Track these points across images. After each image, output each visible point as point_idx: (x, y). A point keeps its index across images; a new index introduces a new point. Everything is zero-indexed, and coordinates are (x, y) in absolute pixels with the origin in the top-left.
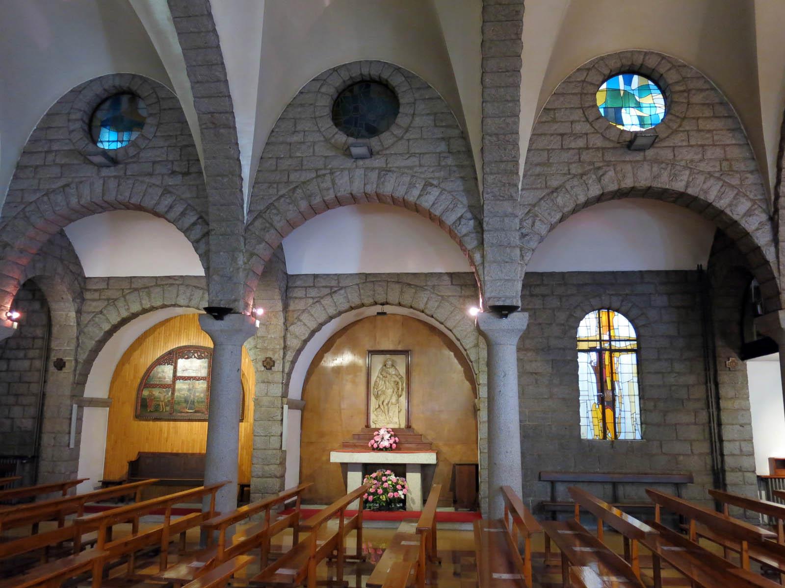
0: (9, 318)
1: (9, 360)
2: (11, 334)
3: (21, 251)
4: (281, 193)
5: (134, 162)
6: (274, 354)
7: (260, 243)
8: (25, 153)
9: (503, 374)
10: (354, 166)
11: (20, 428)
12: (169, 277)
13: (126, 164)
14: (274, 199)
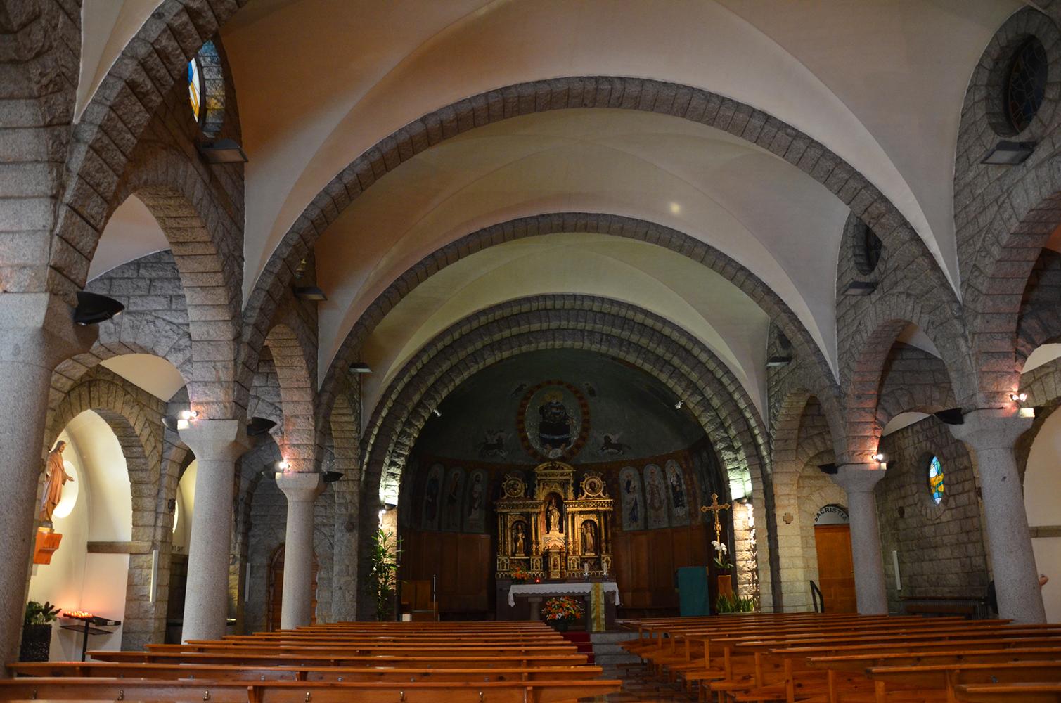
0: (878, 461)
1: (954, 495)
2: (883, 476)
3: (859, 397)
4: (977, 248)
5: (885, 277)
7: (975, 318)
8: (839, 304)
10: (1025, 171)
11: (976, 566)
13: (882, 281)
14: (974, 258)
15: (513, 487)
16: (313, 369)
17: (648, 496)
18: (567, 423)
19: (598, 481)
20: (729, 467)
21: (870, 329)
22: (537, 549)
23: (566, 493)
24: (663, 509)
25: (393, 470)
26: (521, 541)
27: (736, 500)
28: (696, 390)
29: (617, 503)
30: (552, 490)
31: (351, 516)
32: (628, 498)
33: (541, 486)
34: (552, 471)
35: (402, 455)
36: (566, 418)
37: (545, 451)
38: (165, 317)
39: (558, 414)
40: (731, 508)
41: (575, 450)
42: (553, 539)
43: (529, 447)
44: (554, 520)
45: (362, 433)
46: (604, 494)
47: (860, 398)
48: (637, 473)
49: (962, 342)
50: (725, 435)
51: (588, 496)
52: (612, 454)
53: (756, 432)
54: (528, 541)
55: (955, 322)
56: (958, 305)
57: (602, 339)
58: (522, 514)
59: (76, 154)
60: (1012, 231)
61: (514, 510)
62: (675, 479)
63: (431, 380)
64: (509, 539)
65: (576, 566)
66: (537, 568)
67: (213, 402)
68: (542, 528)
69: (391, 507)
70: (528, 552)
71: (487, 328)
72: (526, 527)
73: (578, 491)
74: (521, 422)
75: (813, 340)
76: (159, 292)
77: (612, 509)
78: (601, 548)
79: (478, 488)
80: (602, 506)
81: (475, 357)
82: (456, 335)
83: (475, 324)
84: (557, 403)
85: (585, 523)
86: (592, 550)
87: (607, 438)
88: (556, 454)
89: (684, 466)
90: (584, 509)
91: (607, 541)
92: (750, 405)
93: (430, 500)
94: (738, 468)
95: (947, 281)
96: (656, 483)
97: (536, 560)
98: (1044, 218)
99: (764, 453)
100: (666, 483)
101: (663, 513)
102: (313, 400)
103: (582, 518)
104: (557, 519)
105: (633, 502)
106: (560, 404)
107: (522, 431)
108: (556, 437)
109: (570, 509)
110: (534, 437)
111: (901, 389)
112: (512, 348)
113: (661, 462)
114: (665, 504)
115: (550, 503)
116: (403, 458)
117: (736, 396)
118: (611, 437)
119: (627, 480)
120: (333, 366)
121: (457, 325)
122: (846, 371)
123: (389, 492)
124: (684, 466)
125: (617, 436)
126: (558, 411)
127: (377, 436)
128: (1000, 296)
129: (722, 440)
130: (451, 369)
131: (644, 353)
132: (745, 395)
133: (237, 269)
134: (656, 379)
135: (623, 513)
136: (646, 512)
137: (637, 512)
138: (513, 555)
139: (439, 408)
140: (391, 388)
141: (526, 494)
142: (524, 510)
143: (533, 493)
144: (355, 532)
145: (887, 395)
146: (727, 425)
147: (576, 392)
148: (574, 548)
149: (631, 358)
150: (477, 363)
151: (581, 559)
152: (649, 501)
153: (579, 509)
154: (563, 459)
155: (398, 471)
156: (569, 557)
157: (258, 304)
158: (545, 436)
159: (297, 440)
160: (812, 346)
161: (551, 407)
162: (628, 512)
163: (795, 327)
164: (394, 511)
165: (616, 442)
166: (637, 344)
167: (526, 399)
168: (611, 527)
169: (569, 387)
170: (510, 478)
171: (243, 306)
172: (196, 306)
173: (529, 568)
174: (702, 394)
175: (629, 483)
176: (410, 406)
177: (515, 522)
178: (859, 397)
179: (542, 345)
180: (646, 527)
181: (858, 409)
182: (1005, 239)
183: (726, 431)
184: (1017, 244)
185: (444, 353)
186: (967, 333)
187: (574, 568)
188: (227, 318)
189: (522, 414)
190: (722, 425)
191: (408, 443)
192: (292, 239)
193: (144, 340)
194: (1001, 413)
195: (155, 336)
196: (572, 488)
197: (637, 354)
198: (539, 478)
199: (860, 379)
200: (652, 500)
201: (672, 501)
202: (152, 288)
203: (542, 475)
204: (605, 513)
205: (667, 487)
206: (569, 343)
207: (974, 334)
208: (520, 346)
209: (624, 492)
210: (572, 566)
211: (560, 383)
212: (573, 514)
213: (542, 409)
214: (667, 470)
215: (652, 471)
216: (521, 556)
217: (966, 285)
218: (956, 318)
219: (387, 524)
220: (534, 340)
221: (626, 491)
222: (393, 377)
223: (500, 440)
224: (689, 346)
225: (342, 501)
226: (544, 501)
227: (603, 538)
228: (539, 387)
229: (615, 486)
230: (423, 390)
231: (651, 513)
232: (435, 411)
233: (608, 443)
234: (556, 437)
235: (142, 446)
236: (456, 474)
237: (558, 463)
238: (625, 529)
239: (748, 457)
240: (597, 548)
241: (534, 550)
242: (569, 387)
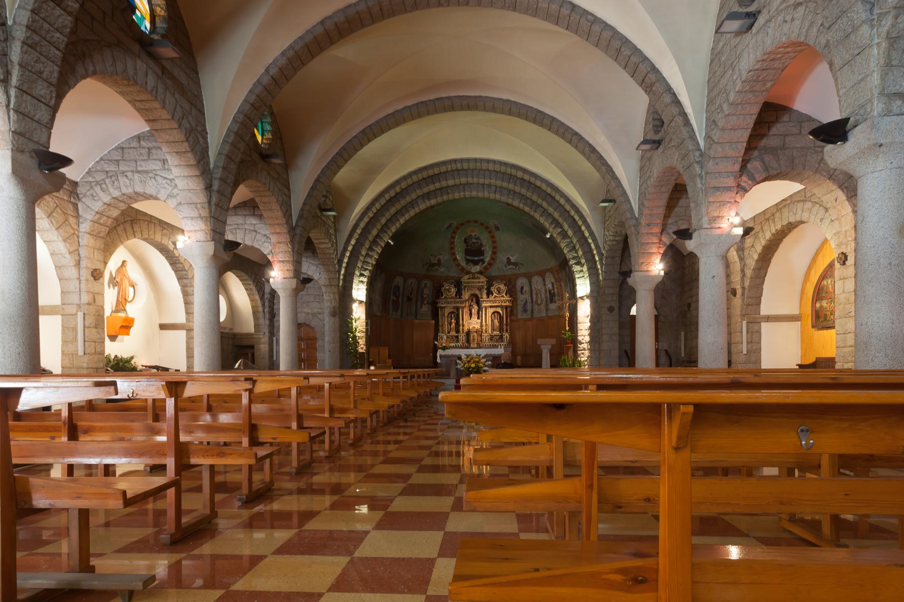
6: (846, 248)
9: (861, 219)
12: (783, 200)
15: (449, 290)
16: (287, 211)
17: (534, 296)
19: (502, 287)
20: (577, 276)
21: (655, 175)
22: (463, 329)
23: (481, 294)
24: (543, 305)
25: (362, 279)
26: (454, 324)
27: (580, 298)
28: (558, 224)
29: (514, 300)
30: (473, 292)
31: (334, 307)
32: (521, 297)
33: (466, 290)
34: (473, 280)
35: (367, 269)
36: (481, 245)
37: (469, 267)
38: (162, 174)
39: (476, 243)
40: (577, 302)
41: (488, 267)
42: (472, 323)
43: (459, 265)
44: (474, 311)
45: (339, 255)
46: (506, 294)
47: (650, 225)
48: (527, 281)
49: (698, 180)
50: (576, 255)
51: (495, 296)
53: (595, 252)
54: (457, 324)
55: (696, 165)
56: (699, 152)
57: (496, 190)
58: (454, 307)
59: (14, 48)
60: (736, 90)
61: (449, 305)
62: (551, 285)
63: (383, 221)
64: (446, 323)
67: (198, 231)
68: (466, 317)
69: (361, 302)
70: (458, 331)
71: (419, 184)
72: (456, 315)
73: (489, 293)
74: (452, 248)
75: (622, 185)
76: (155, 157)
77: (511, 305)
78: (503, 329)
79: (426, 291)
81: (412, 204)
82: (398, 189)
83: (410, 181)
85: (494, 313)
87: (508, 259)
88: (476, 269)
89: (557, 277)
90: (493, 305)
91: (507, 325)
92: (592, 234)
93: (395, 299)
94: (583, 276)
95: (695, 133)
96: (539, 288)
97: (462, 337)
98: (761, 78)
99: (599, 267)
100: (545, 288)
101: (543, 307)
102: (289, 232)
103: (492, 310)
104: (476, 310)
107: (454, 254)
108: (476, 258)
109: (484, 305)
111: (683, 219)
112: (436, 198)
113: (542, 274)
114: (544, 302)
115: (472, 300)
116: (368, 271)
117: (583, 228)
118: (511, 258)
119: (521, 286)
120: (302, 210)
121: (398, 182)
122: (641, 207)
123: (359, 291)
124: (557, 277)
125: (515, 258)
127: (349, 257)
128: (728, 144)
129: (574, 258)
130: (396, 213)
131: (524, 199)
132: (588, 227)
133: (201, 139)
134: (533, 217)
136: (532, 307)
138: (449, 333)
139: (391, 238)
140: (356, 226)
141: (456, 295)
142: (455, 305)
143: (461, 295)
144: (337, 317)
145: (672, 224)
146: (577, 248)
147: (487, 228)
148: (486, 329)
149: (516, 203)
150: (414, 208)
152: (534, 300)
153: (490, 304)
154: (481, 273)
155: (365, 280)
156: (483, 334)
157: (221, 164)
158: (470, 258)
159: (282, 258)
160: (621, 189)
161: (472, 238)
163: (610, 176)
164: (364, 305)
166: (519, 193)
167: (455, 233)
168: (510, 317)
169: (482, 224)
171: (211, 166)
172: (176, 166)
173: (458, 341)
174: (561, 227)
175: (522, 288)
176: (371, 238)
177: (450, 313)
178: (649, 225)
179: (457, 196)
180: (532, 316)
181: (647, 233)
182: (732, 97)
183: (576, 252)
184: (742, 101)
185: (391, 201)
186: (703, 173)
188: (198, 174)
189: (452, 243)
190: (574, 248)
191: (371, 262)
192: (239, 118)
193: (150, 190)
194: (718, 232)
195: (157, 188)
196: (485, 291)
197: (519, 200)
199: (649, 212)
200: (537, 299)
201: (549, 300)
202: (151, 155)
204: (506, 307)
205: (546, 291)
206: (474, 194)
207: (707, 174)
208: (442, 196)
209: (519, 294)
211: (476, 222)
212: (486, 308)
213: (465, 239)
214: (546, 279)
215: (536, 279)
216: (453, 333)
217: (708, 137)
218: (697, 162)
219: (359, 313)
220: (451, 192)
221: (520, 293)
222: (357, 217)
223: (439, 260)
224: (553, 194)
225: (328, 298)
226: (468, 300)
227: (505, 322)
228: (462, 224)
229: (514, 290)
230: (379, 227)
231: (536, 307)
232: (390, 241)
233: (509, 262)
234: (476, 258)
235: (182, 263)
236: (411, 283)
237: (477, 275)
238: (520, 317)
239: (589, 269)
240: (501, 329)
241: (461, 330)
242: (482, 224)
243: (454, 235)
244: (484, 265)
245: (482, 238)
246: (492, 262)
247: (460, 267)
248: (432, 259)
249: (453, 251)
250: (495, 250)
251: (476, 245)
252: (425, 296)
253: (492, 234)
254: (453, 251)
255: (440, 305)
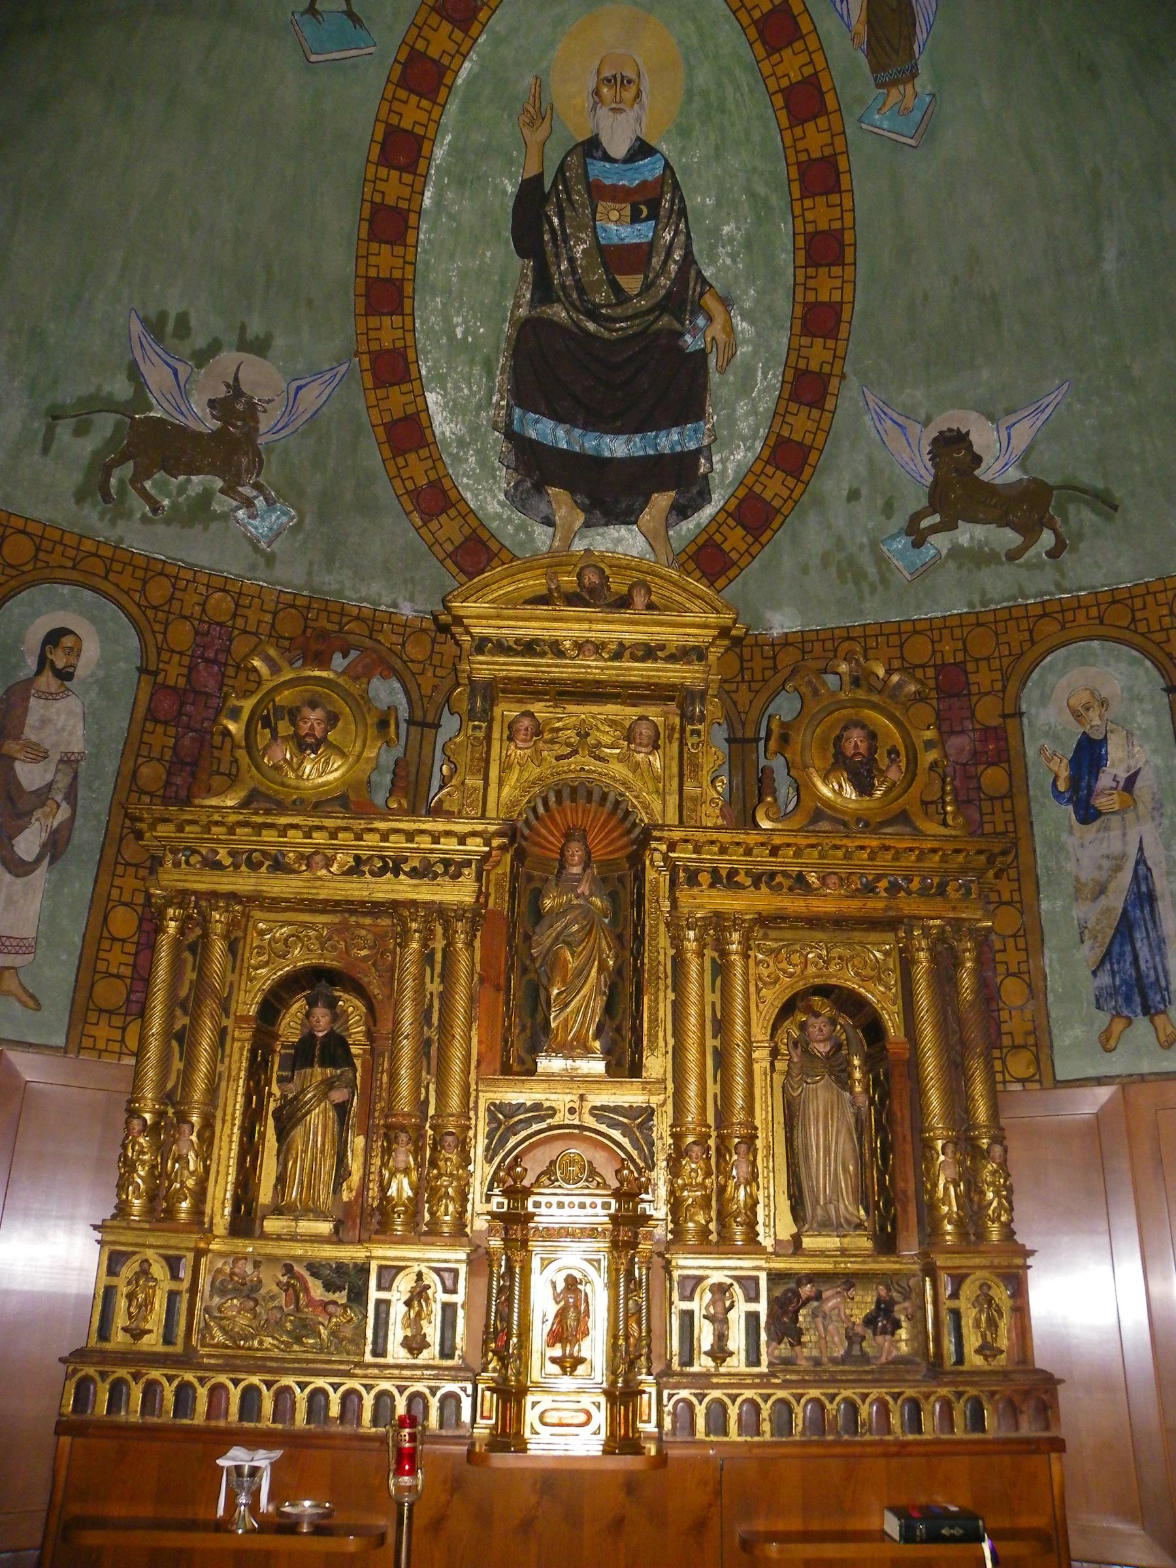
18: (690, 342)
37: (542, 536)
41: (735, 538)
52: (979, 558)
65: (737, 1340)
66: (414, 1344)
80: (924, 892)
84: (641, 150)
86: (849, 1208)
105: (1126, 877)
106: (650, 169)
108: (617, 447)
110: (474, 429)
125: (1023, 435)
126: (642, 233)
135: (1050, 959)
137: (1159, 946)
151: (775, 1277)
162: (1088, 953)
165: (1013, 474)
170: (288, 675)
187: (720, 1352)
198: (485, 667)
203: (501, 648)
210: (705, 1336)
229: (993, 778)
234: (617, 447)
243: (411, 115)
244: (689, 526)
245: (699, 200)
246: (774, 488)
247: (449, 529)
248: (156, 375)
249: (387, 332)
250: (818, 354)
251: (631, 283)
252: (30, 775)
253: (815, 139)
254: (387, 332)
255: (171, 878)
